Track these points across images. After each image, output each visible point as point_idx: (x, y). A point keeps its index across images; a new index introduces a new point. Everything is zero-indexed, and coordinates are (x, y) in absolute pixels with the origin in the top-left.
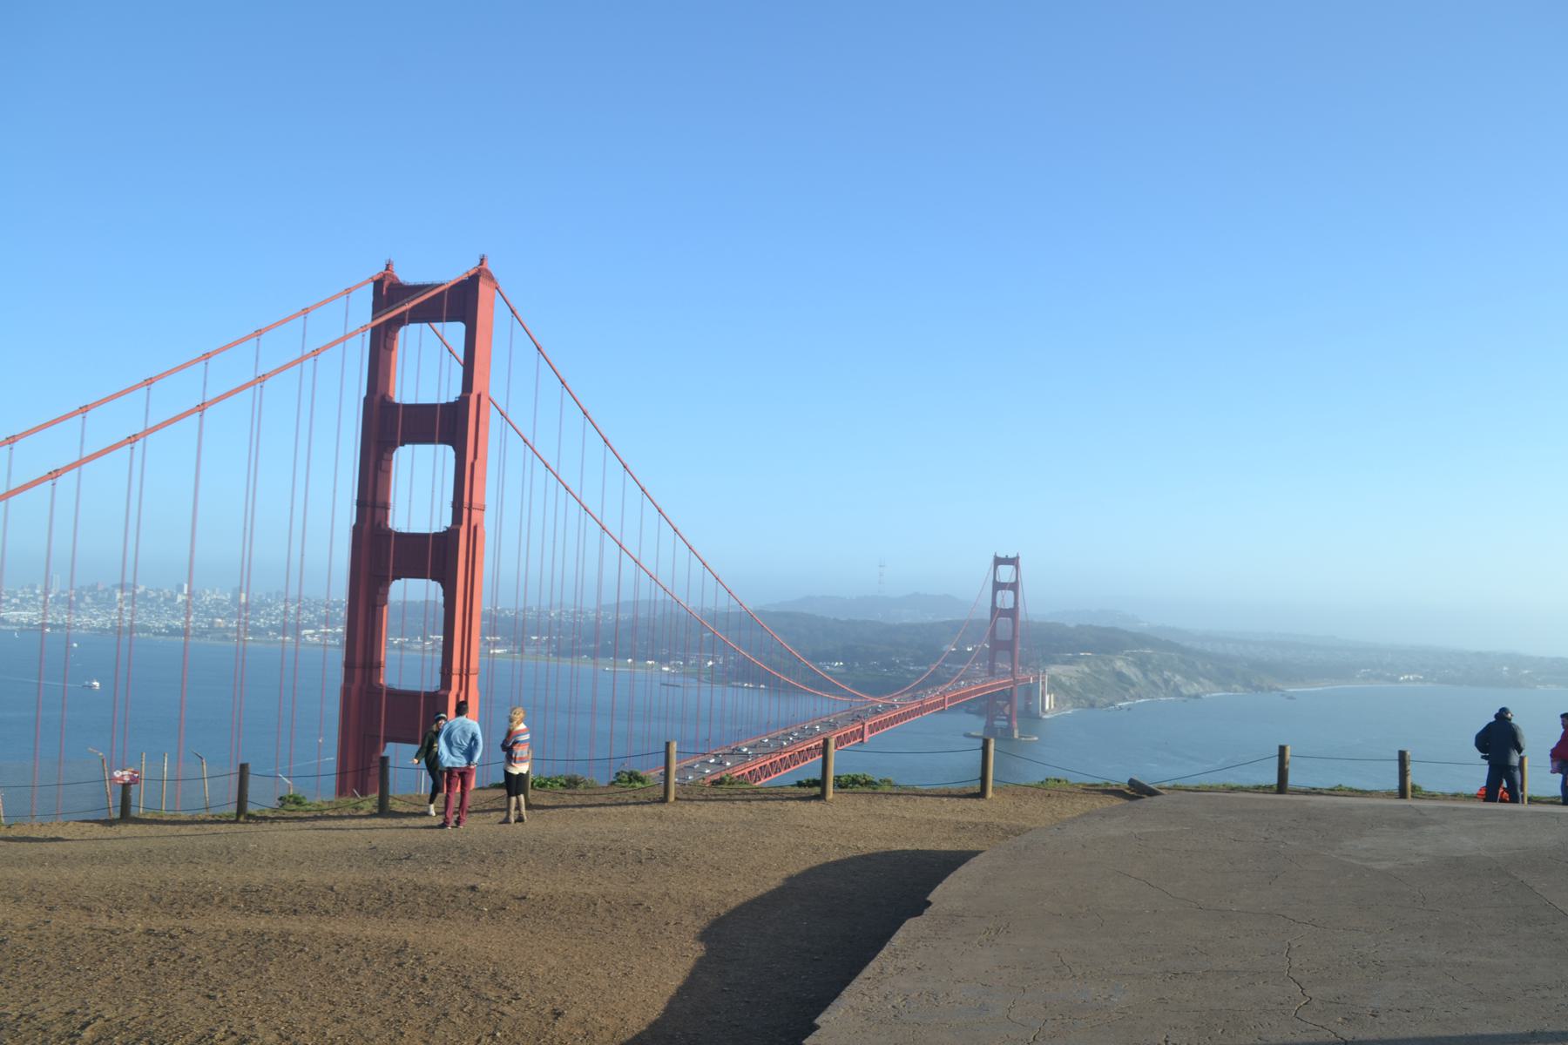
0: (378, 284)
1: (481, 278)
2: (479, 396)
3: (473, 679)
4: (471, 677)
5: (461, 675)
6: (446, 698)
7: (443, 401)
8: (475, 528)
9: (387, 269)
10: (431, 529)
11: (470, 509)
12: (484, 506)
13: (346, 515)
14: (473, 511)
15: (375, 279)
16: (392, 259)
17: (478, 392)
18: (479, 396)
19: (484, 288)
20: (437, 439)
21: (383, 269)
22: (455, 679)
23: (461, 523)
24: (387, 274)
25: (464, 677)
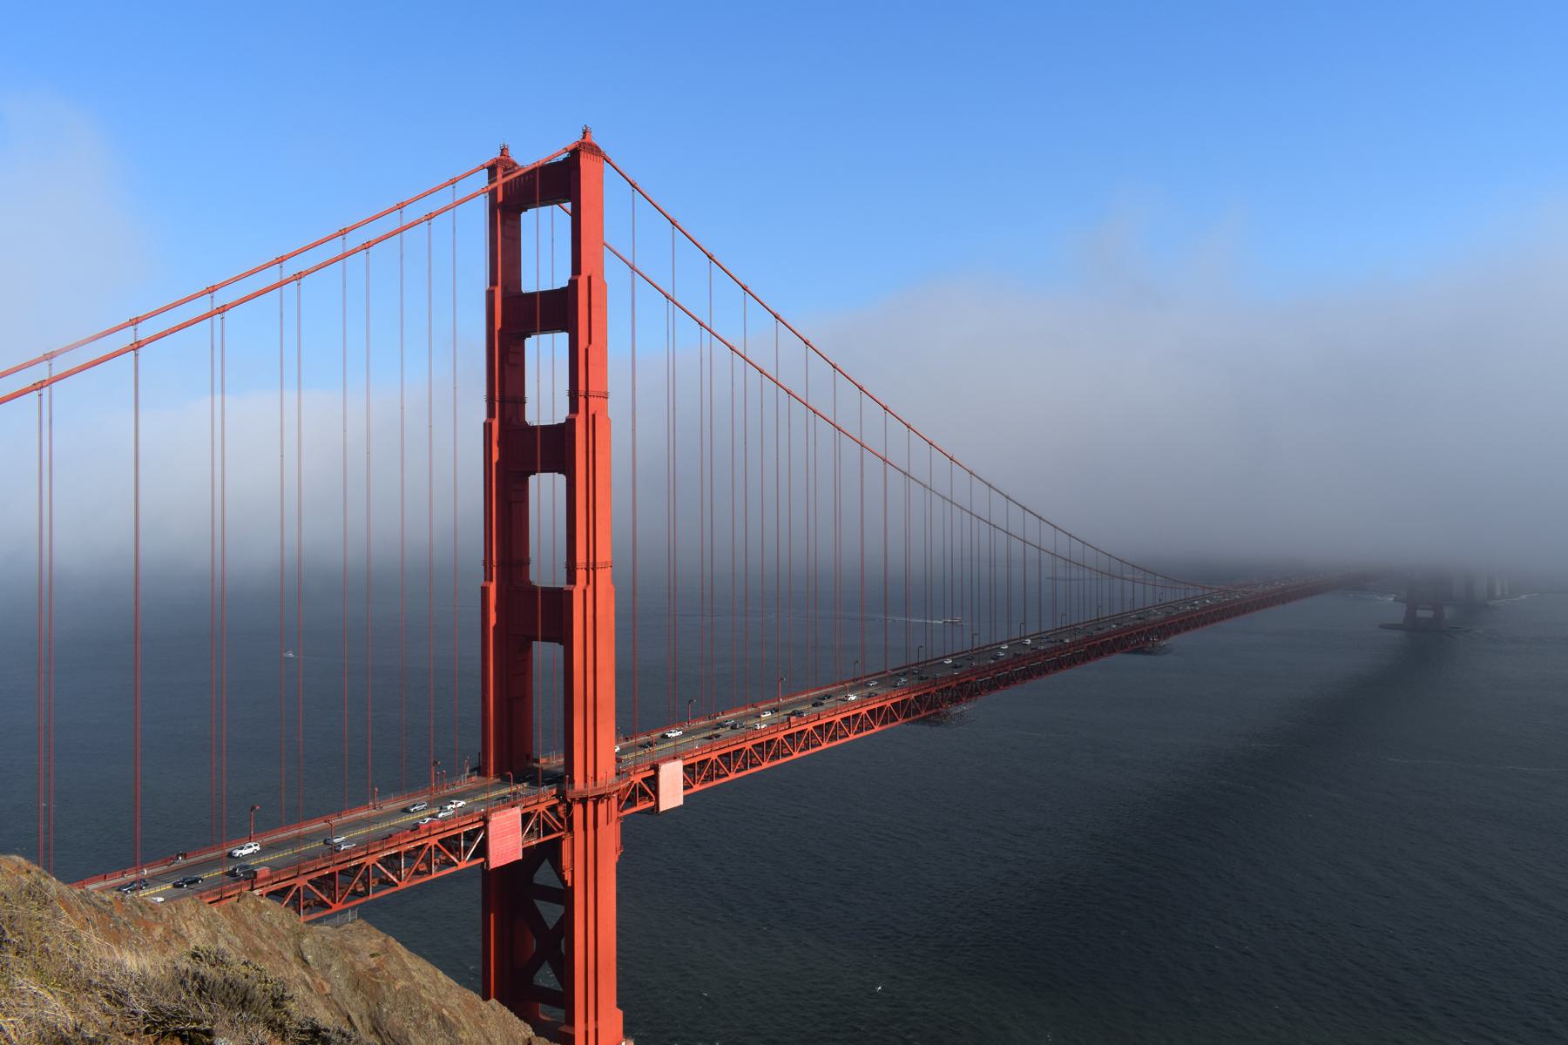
0: (492, 169)
1: (582, 153)
2: (589, 278)
3: (603, 576)
4: (598, 571)
5: (587, 569)
6: (571, 593)
7: (557, 287)
8: (594, 416)
9: (502, 154)
10: (553, 420)
11: (586, 398)
12: (606, 393)
13: (476, 410)
14: (590, 399)
15: (488, 164)
16: (506, 144)
17: (589, 274)
18: (589, 278)
19: (586, 162)
20: (538, 328)
21: (498, 156)
22: (581, 574)
23: (577, 412)
24: (502, 160)
25: (591, 572)
